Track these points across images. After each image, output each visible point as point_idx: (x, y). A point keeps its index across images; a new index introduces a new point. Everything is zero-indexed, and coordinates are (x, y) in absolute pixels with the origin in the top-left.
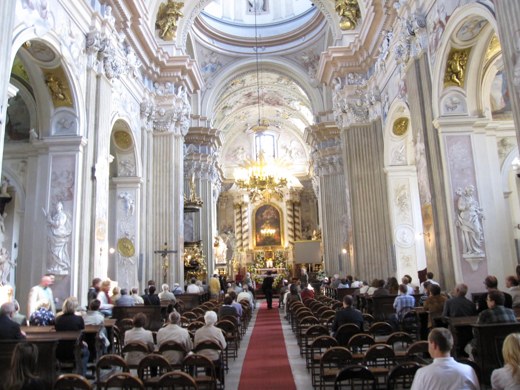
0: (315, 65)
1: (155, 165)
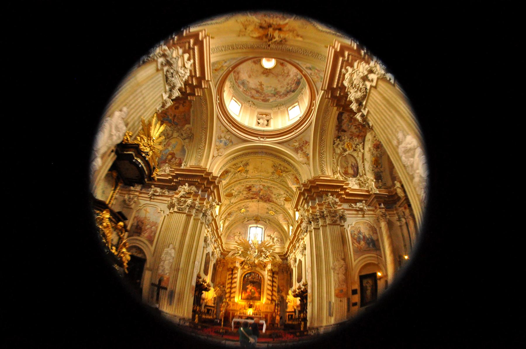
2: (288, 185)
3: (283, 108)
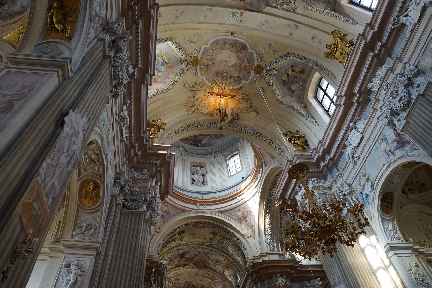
0: (248, 218)
1: (117, 243)
2: (229, 252)
3: (219, 157)
